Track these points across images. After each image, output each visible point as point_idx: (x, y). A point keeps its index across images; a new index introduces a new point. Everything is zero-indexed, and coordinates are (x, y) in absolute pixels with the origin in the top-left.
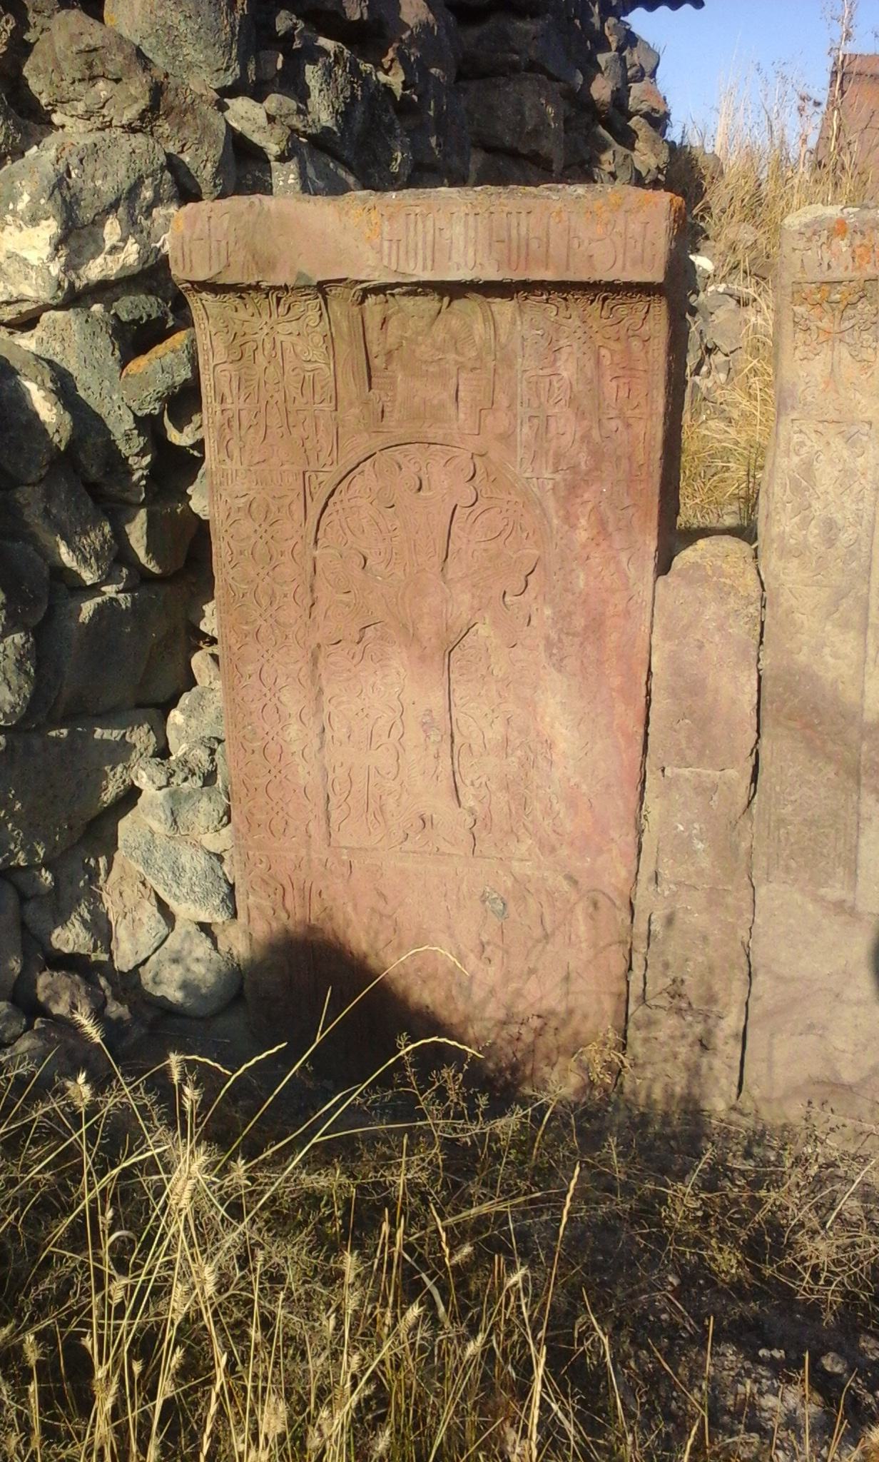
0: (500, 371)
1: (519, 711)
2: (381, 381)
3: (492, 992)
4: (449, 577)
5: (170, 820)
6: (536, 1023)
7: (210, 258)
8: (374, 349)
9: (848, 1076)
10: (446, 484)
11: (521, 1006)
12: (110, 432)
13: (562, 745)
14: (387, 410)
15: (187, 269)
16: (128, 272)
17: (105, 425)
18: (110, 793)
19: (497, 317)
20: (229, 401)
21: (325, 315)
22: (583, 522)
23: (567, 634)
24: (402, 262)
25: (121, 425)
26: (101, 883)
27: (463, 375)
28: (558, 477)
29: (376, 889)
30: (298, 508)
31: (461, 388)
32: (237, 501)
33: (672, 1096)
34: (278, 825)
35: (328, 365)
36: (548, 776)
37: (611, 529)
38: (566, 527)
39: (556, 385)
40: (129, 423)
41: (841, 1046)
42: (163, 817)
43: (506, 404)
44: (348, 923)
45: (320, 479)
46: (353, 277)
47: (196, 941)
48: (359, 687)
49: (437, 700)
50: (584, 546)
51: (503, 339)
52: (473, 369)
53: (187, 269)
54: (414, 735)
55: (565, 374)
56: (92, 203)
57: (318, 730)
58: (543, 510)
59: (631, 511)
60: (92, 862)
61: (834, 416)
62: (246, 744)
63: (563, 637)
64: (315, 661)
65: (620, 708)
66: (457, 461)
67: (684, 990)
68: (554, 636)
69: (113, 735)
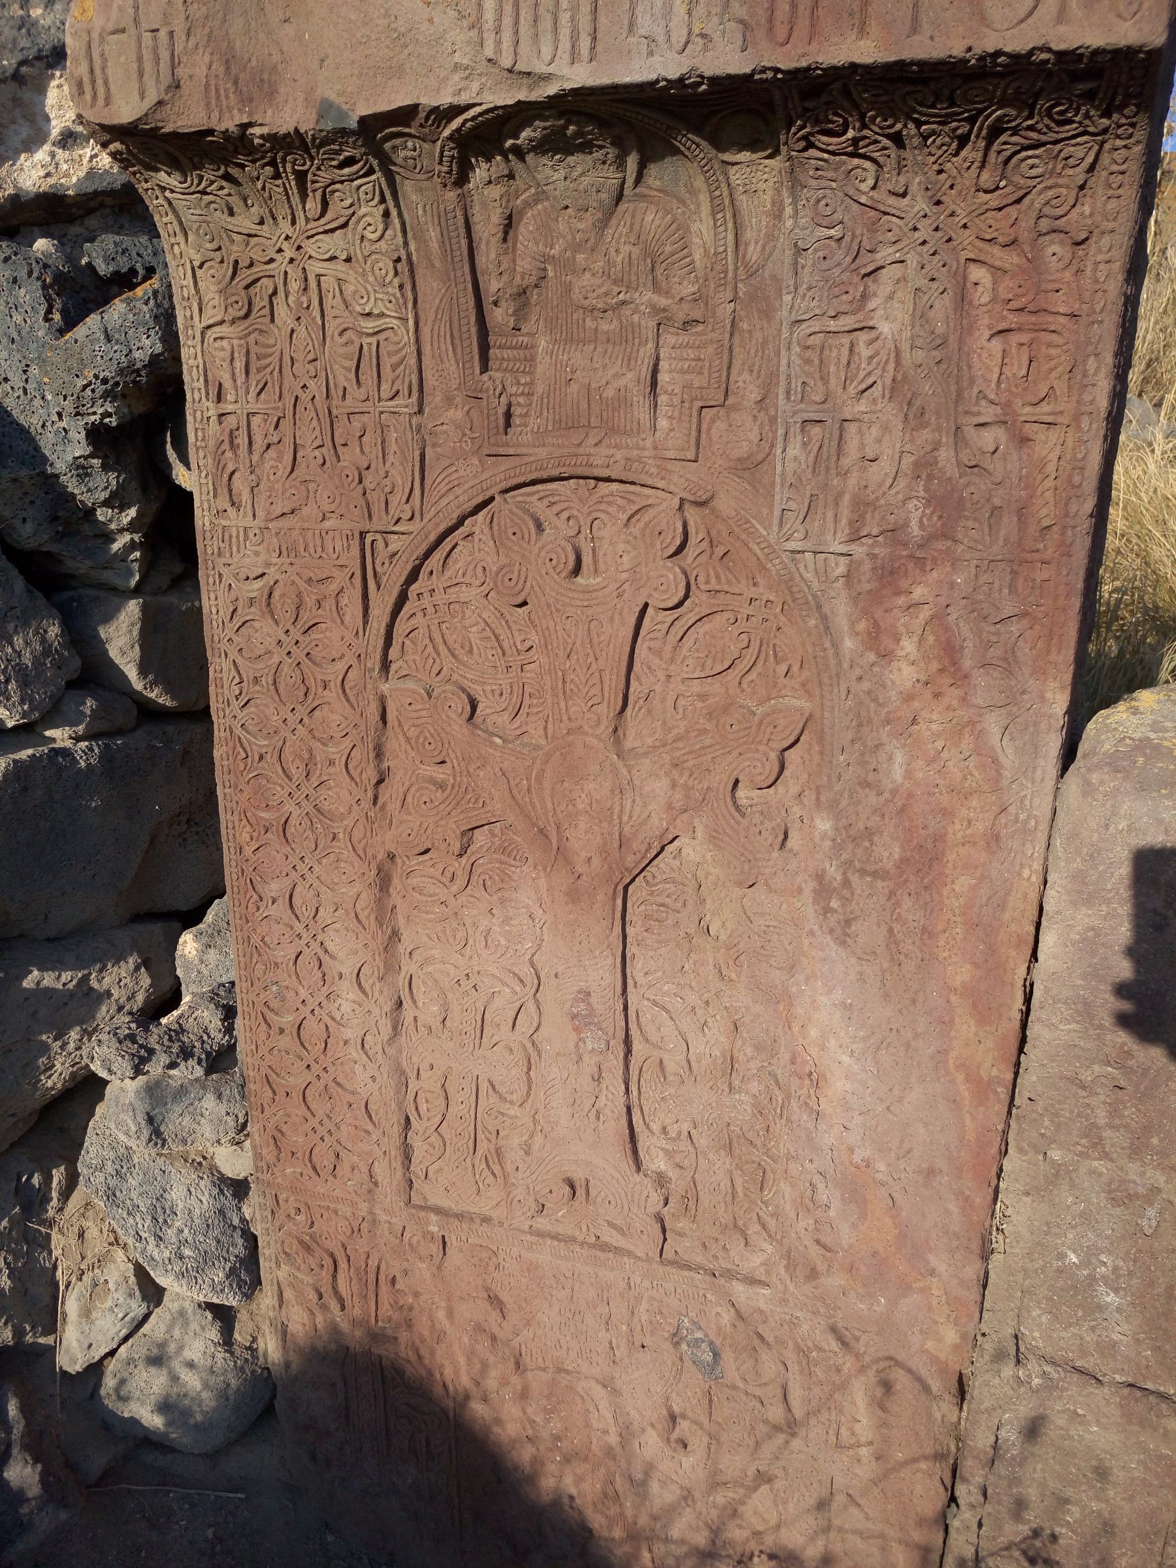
0: (745, 326)
1: (758, 1009)
2: (506, 353)
3: (687, 1496)
4: (628, 744)
5: (146, 1133)
7: (141, 75)
8: (492, 286)
10: (627, 560)
11: (736, 1533)
12: (44, 459)
13: (839, 1085)
14: (517, 411)
15: (101, 101)
16: (101, 185)
17: (37, 448)
18: (55, 1079)
19: (742, 200)
20: (230, 397)
21: (394, 212)
22: (908, 646)
23: (863, 872)
24: (524, 47)
25: (66, 449)
26: (51, 1213)
27: (670, 339)
29: (487, 1289)
30: (352, 602)
31: (663, 365)
32: (248, 586)
34: (324, 1158)
35: (404, 320)
36: (810, 1139)
37: (967, 663)
38: (871, 657)
39: (864, 351)
40: (79, 447)
42: (133, 1129)
43: (755, 396)
44: (440, 1337)
45: (392, 547)
46: (428, 100)
47: (194, 1326)
48: (460, 935)
49: (600, 974)
50: (908, 698)
51: (753, 253)
52: (688, 324)
53: (101, 101)
54: (556, 1034)
55: (885, 328)
56: (14, 41)
57: (387, 1007)
58: (824, 618)
59: (1014, 628)
60: (36, 1180)
62: (270, 1016)
63: (854, 878)
64: (384, 881)
65: (966, 1026)
66: (651, 513)
68: (834, 873)
69: (63, 980)
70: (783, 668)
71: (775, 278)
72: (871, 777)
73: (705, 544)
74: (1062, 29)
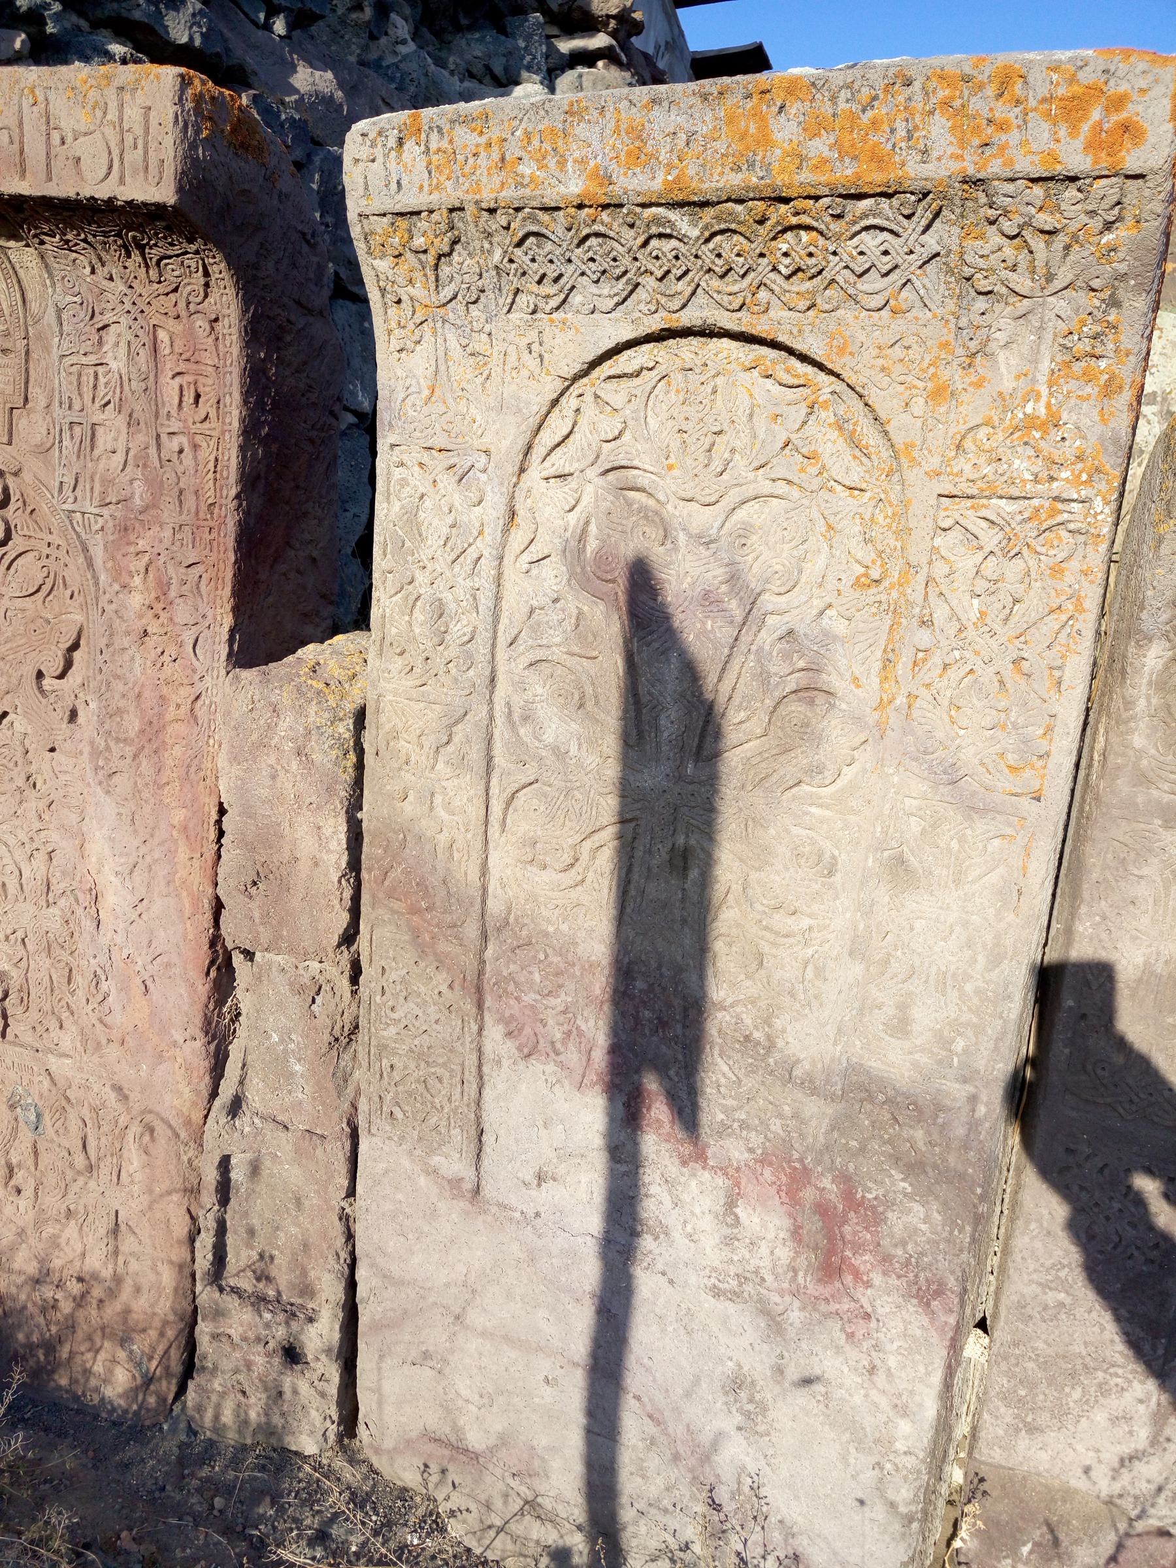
6: (75, 1288)
9: (475, 1439)
22: (137, 581)
23: (118, 740)
28: (105, 511)
33: (246, 1422)
41: (465, 1393)
43: (43, 404)
55: (114, 365)
61: (441, 441)
63: (112, 744)
65: (183, 853)
67: (274, 1272)
70: (69, 593)
71: (49, 325)
72: (119, 671)
73: (20, 503)
74: (122, 188)
